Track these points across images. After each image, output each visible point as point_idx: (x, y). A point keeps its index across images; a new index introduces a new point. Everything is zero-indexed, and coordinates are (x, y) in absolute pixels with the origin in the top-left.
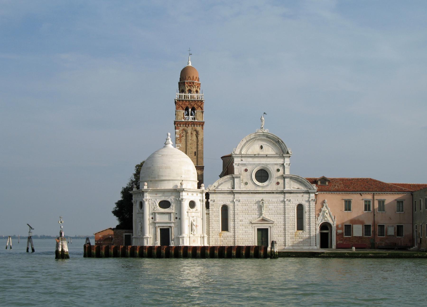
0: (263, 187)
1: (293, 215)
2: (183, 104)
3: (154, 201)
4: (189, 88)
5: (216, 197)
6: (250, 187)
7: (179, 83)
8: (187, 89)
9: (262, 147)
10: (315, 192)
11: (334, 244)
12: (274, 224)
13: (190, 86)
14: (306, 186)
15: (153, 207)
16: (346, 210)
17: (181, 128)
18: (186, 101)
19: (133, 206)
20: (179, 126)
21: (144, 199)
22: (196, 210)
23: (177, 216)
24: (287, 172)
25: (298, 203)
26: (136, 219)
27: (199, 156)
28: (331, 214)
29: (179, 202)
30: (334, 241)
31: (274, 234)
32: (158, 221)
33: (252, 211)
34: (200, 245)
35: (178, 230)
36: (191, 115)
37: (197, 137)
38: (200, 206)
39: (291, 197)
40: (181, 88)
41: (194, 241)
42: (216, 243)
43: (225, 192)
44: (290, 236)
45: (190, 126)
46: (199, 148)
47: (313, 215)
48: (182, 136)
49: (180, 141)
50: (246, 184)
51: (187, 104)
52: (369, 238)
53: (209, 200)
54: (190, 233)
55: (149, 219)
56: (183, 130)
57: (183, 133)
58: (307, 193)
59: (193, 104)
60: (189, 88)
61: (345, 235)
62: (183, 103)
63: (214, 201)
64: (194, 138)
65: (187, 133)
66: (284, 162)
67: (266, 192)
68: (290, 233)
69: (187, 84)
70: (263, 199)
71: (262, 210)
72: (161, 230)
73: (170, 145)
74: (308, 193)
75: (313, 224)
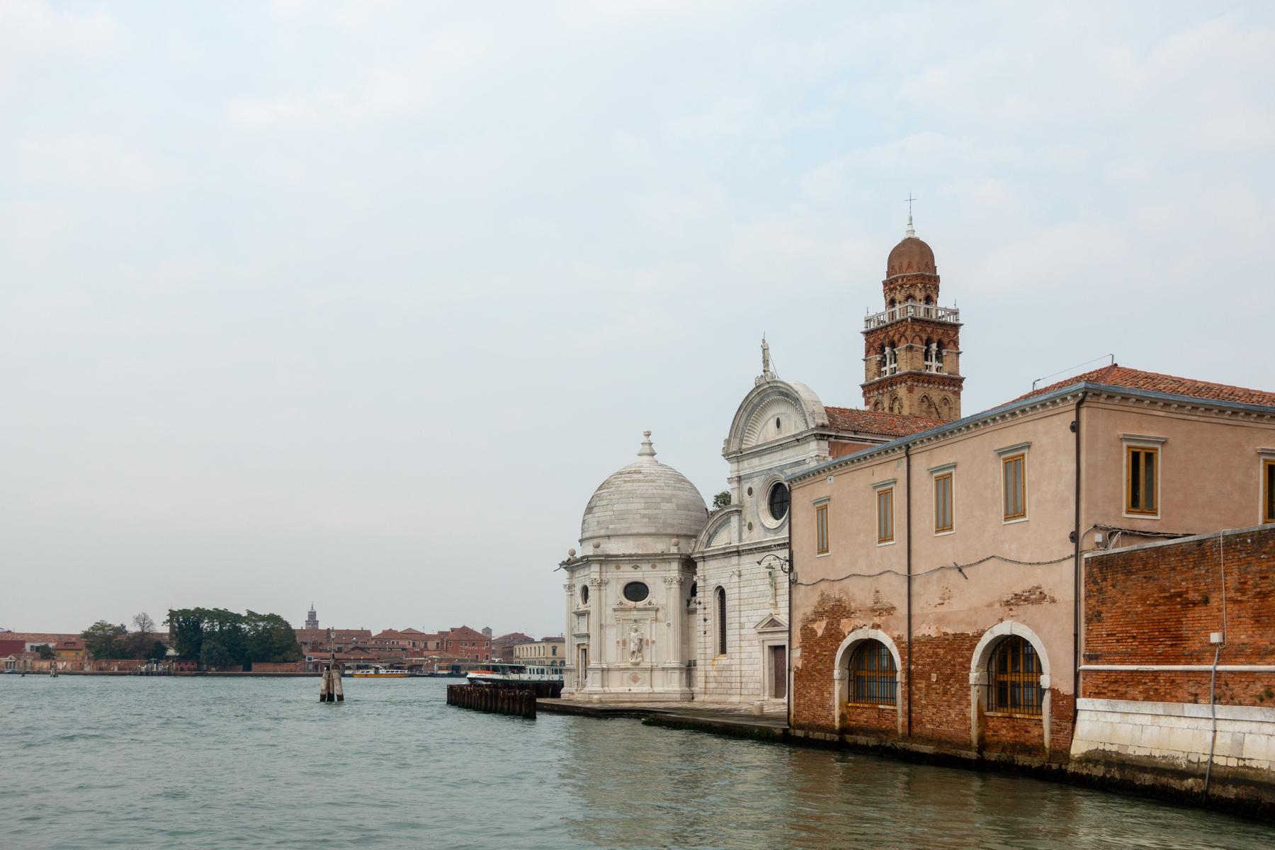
9: (778, 423)
22: (646, 605)
50: (750, 527)
67: (778, 545)
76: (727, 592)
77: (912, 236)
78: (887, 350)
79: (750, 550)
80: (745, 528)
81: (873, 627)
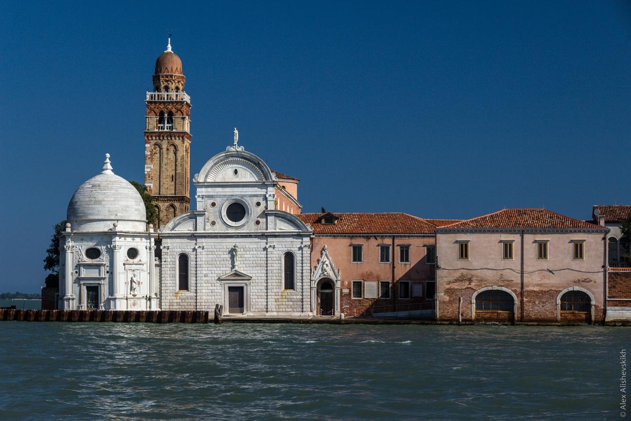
1: (278, 267)
3: (80, 249)
4: (166, 84)
5: (171, 243)
6: (219, 228)
7: (153, 76)
8: (163, 86)
9: (236, 172)
10: (310, 235)
12: (251, 281)
13: (167, 81)
14: (298, 227)
15: (78, 257)
17: (153, 142)
20: (150, 138)
21: (65, 246)
24: (271, 206)
25: (286, 250)
27: (177, 182)
28: (334, 266)
29: (111, 252)
32: (83, 276)
34: (145, 310)
36: (168, 123)
37: (175, 154)
38: (145, 255)
39: (276, 242)
41: (134, 305)
42: (171, 307)
45: (165, 138)
46: (177, 169)
47: (307, 267)
48: (155, 154)
49: (152, 161)
50: (213, 223)
52: (387, 300)
53: (161, 247)
54: (129, 293)
55: (72, 273)
56: (156, 144)
57: (155, 149)
59: (170, 107)
60: (166, 84)
61: (354, 297)
63: (168, 249)
64: (171, 155)
65: (161, 149)
66: (267, 193)
68: (274, 294)
69: (163, 79)
71: (235, 260)
73: (109, 172)
75: (306, 280)
76: (192, 257)
78: (166, 115)
80: (208, 224)
81: (499, 286)
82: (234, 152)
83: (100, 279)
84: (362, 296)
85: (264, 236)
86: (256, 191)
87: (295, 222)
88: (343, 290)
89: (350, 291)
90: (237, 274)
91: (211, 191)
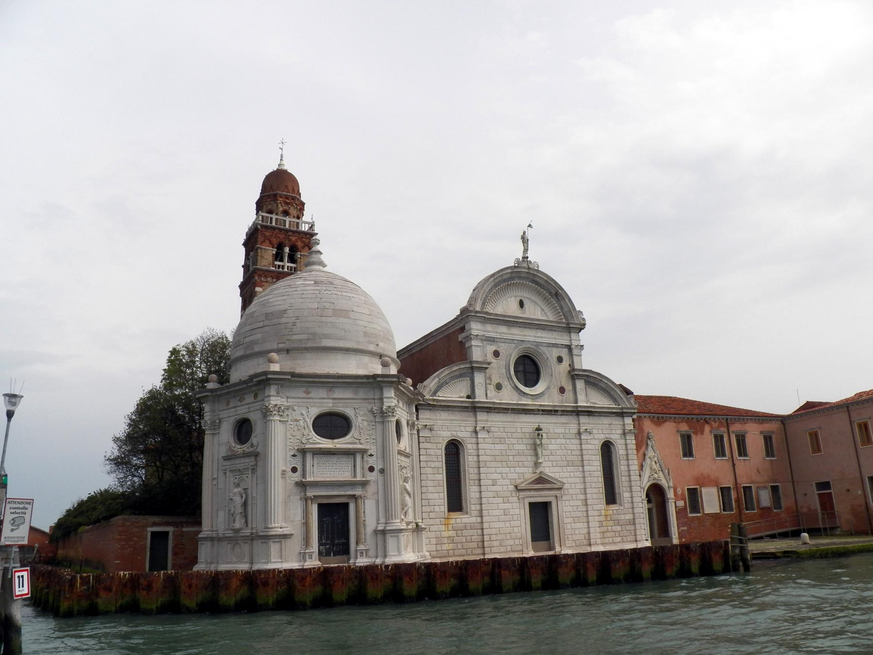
0: (535, 397)
2: (272, 235)
3: (302, 414)
6: (508, 397)
8: (281, 209)
11: (675, 535)
16: (685, 455)
18: (280, 230)
19: (206, 437)
23: (371, 462)
25: (602, 438)
26: (215, 476)
30: (674, 527)
31: (565, 516)
33: (515, 457)
35: (378, 507)
40: (267, 207)
43: (454, 407)
44: (597, 519)
47: (635, 467)
50: (499, 387)
51: (281, 238)
58: (617, 416)
59: (293, 239)
61: (691, 512)
62: (273, 233)
67: (543, 410)
69: (281, 199)
70: (539, 426)
72: (320, 506)
74: (620, 416)
77: (280, 168)
78: (287, 250)
79: (506, 409)
80: (491, 388)
82: (524, 268)
83: (353, 484)
84: (701, 510)
85: (577, 412)
86: (555, 339)
87: (612, 393)
88: (677, 502)
89: (685, 503)
90: (541, 480)
91: (491, 330)
